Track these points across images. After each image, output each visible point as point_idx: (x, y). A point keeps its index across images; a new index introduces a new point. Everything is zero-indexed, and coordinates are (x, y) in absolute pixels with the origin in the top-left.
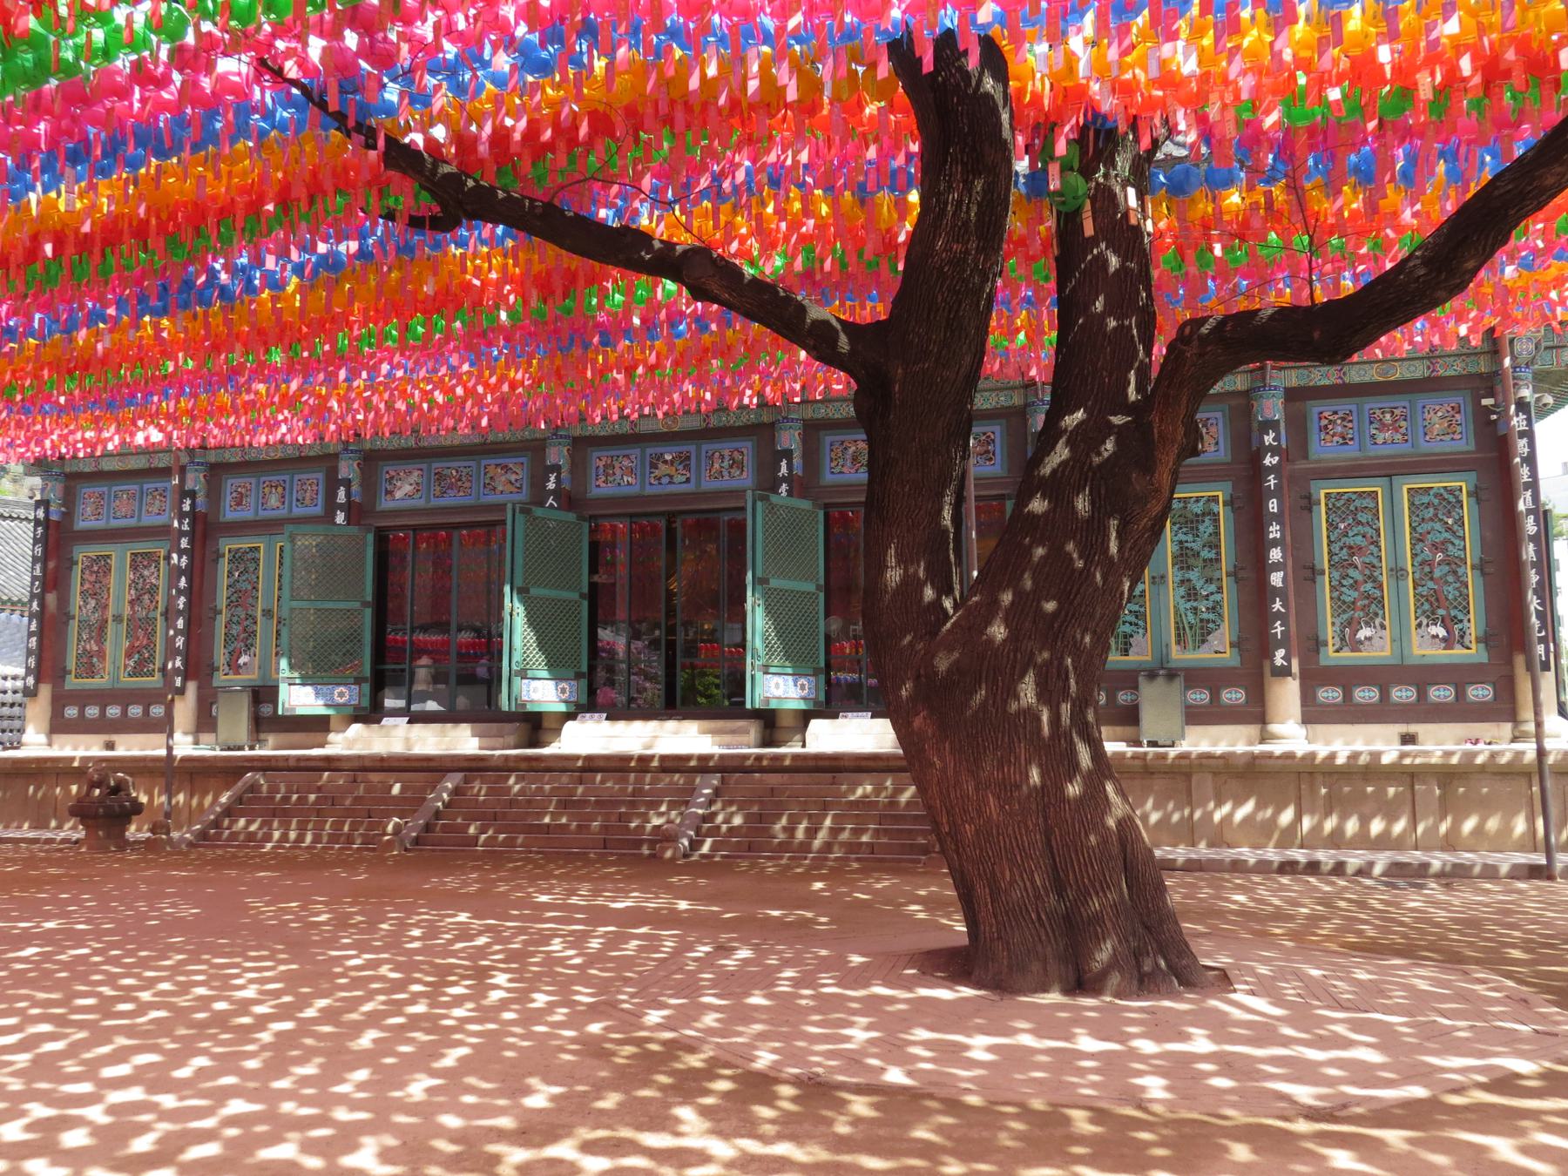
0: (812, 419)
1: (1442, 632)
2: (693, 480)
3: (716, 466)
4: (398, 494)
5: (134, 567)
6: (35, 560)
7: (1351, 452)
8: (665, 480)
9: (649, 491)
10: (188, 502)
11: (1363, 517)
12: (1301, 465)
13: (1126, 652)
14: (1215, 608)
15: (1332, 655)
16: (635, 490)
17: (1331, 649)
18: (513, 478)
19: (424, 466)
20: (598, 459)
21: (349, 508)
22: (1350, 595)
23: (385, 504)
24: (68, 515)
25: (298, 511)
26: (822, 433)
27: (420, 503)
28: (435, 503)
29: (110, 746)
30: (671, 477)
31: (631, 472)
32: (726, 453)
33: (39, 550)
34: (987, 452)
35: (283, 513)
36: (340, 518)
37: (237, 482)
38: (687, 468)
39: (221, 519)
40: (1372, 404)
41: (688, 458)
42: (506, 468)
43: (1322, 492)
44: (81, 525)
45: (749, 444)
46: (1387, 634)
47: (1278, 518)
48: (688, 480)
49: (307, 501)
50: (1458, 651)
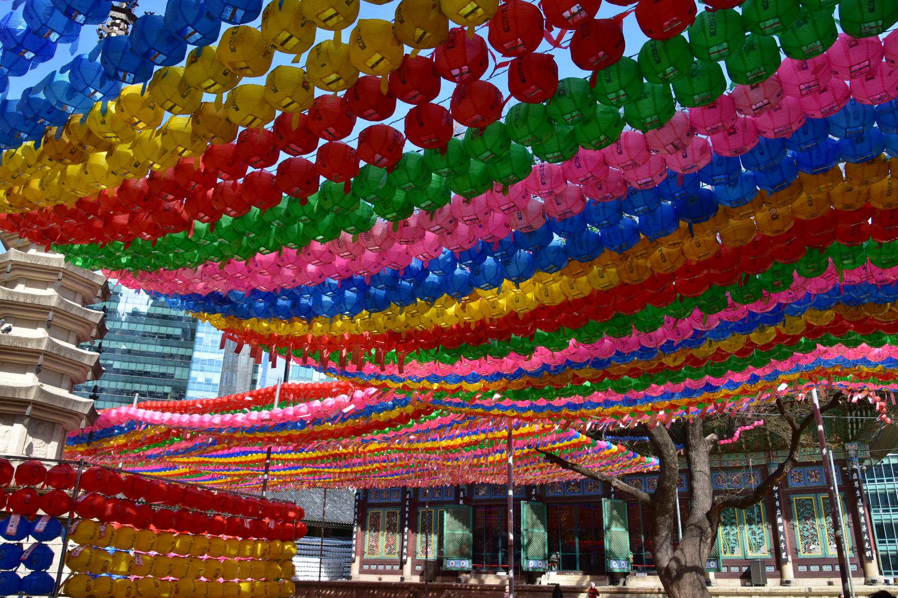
5: (388, 516)
6: (355, 513)
7: (802, 485)
9: (567, 495)
11: (808, 507)
12: (786, 489)
13: (733, 553)
15: (802, 555)
16: (562, 495)
17: (801, 552)
21: (464, 499)
23: (475, 497)
24: (365, 499)
25: (445, 499)
28: (493, 497)
29: (380, 579)
33: (356, 510)
35: (440, 499)
36: (461, 502)
40: (807, 469)
43: (794, 498)
44: (370, 501)
47: (780, 508)
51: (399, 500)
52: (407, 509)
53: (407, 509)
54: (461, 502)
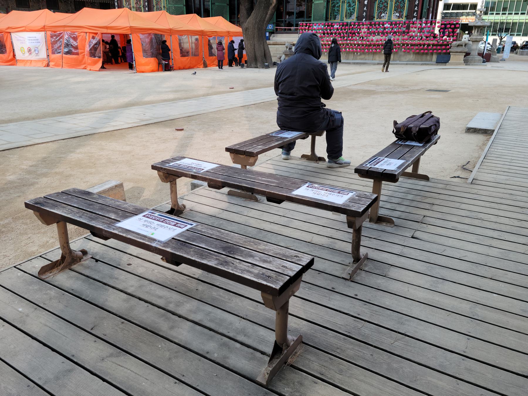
1: (398, 15)
14: (354, 9)
15: (376, 20)
22: (381, 6)
46: (387, 15)
50: (401, 19)
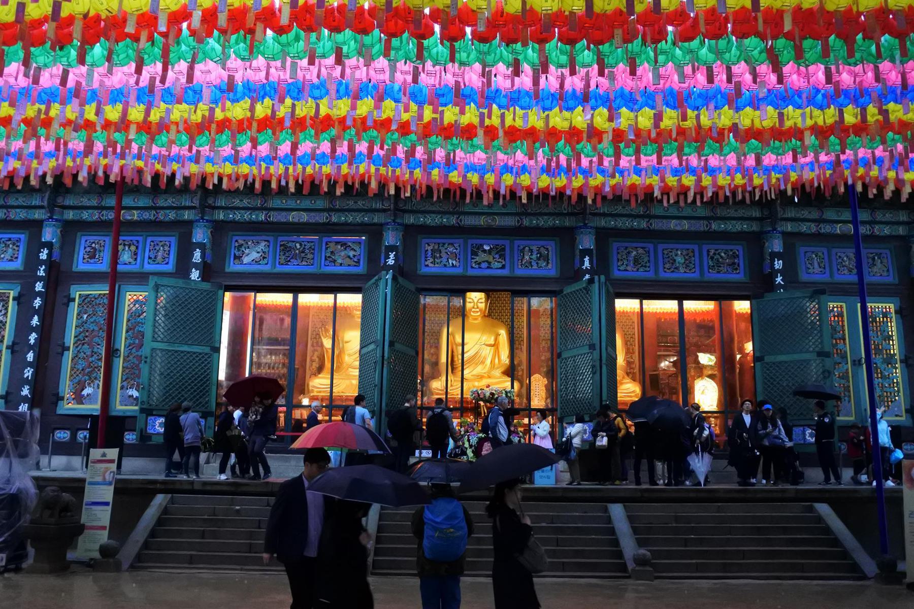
0: (604, 228)
2: (507, 266)
3: (527, 257)
4: (246, 260)
8: (484, 265)
9: (471, 273)
10: (46, 251)
16: (458, 271)
18: (351, 253)
19: (271, 239)
20: (428, 245)
25: (149, 267)
26: (610, 239)
27: (267, 269)
28: (279, 269)
30: (489, 263)
31: (455, 256)
32: (535, 248)
34: (734, 263)
36: (195, 275)
37: (92, 239)
38: (502, 256)
39: (74, 269)
41: (504, 250)
42: (345, 245)
45: (552, 243)
48: (503, 267)
49: (159, 258)
51: (17, 265)
52: (39, 287)
53: (39, 287)
54: (195, 275)
